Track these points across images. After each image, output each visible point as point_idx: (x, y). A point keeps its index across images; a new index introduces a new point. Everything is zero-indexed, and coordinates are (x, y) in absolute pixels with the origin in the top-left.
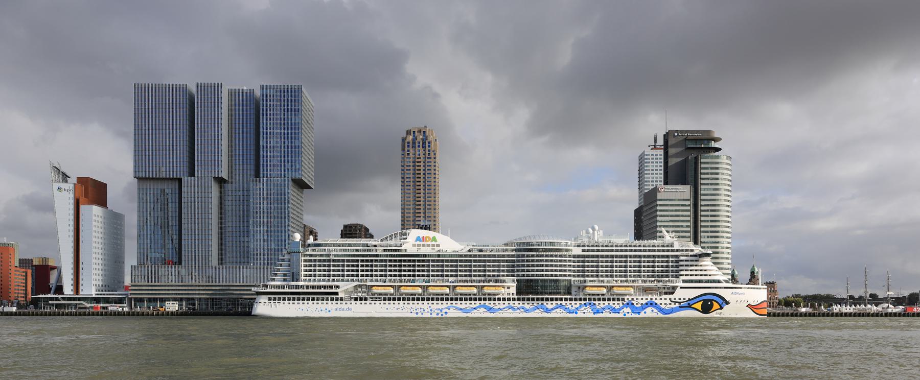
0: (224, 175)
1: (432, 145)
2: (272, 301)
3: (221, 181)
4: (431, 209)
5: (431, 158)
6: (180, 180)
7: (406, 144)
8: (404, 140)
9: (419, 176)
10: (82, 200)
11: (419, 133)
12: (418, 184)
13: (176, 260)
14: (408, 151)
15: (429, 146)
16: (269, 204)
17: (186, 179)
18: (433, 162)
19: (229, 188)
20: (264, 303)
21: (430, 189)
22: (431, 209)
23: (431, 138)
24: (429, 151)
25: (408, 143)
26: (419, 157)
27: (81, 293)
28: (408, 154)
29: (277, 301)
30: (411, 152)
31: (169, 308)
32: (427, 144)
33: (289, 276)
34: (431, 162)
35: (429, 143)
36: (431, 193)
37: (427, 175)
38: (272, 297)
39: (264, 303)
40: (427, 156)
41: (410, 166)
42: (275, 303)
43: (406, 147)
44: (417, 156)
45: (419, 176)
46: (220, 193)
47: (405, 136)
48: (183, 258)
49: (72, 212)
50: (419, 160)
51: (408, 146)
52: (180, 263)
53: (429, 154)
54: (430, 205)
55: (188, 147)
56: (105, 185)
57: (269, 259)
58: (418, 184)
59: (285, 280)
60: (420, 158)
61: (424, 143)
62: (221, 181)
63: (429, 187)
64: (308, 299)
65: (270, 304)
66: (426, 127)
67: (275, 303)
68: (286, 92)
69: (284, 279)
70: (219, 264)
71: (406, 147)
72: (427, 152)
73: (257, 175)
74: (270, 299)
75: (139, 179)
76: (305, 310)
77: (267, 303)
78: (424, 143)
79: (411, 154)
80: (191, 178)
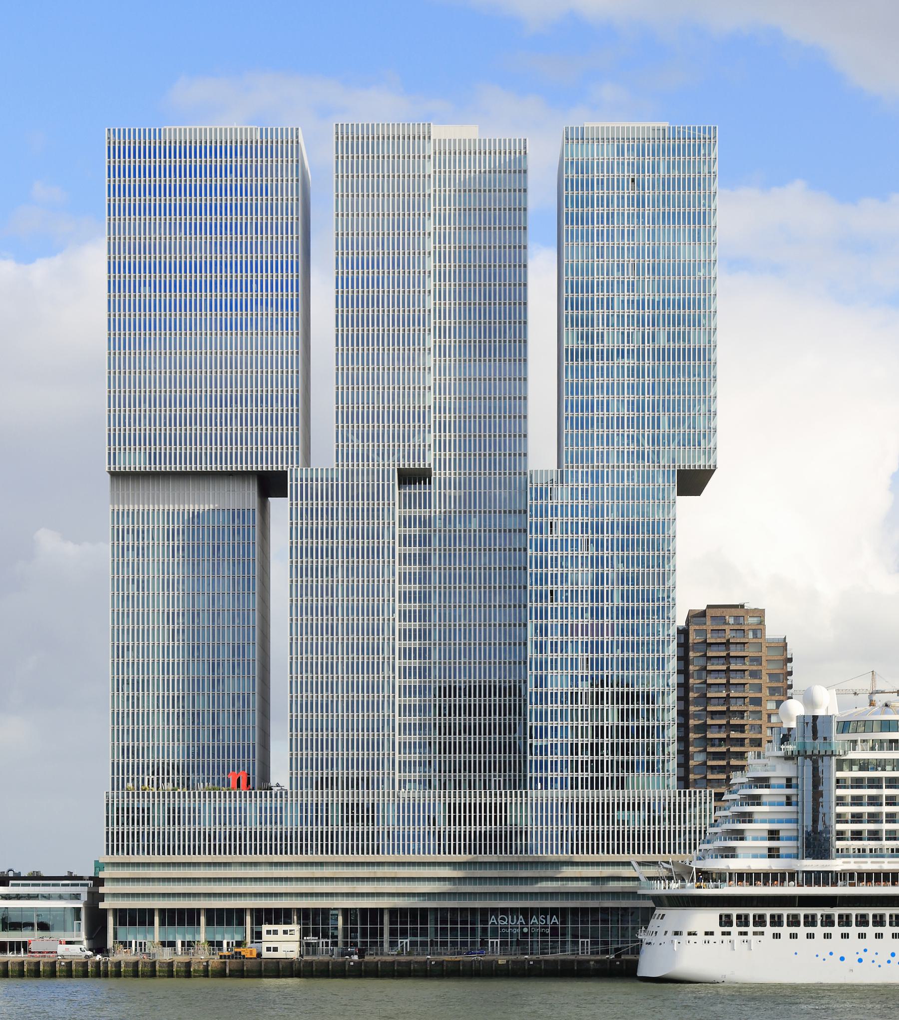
2: (735, 929)
20: (707, 933)
29: (751, 929)
31: (275, 949)
33: (789, 839)
38: (734, 912)
39: (707, 933)
42: (745, 933)
59: (773, 853)
64: (862, 921)
65: (726, 938)
67: (745, 933)
69: (770, 849)
74: (725, 921)
76: (851, 960)
77: (718, 936)
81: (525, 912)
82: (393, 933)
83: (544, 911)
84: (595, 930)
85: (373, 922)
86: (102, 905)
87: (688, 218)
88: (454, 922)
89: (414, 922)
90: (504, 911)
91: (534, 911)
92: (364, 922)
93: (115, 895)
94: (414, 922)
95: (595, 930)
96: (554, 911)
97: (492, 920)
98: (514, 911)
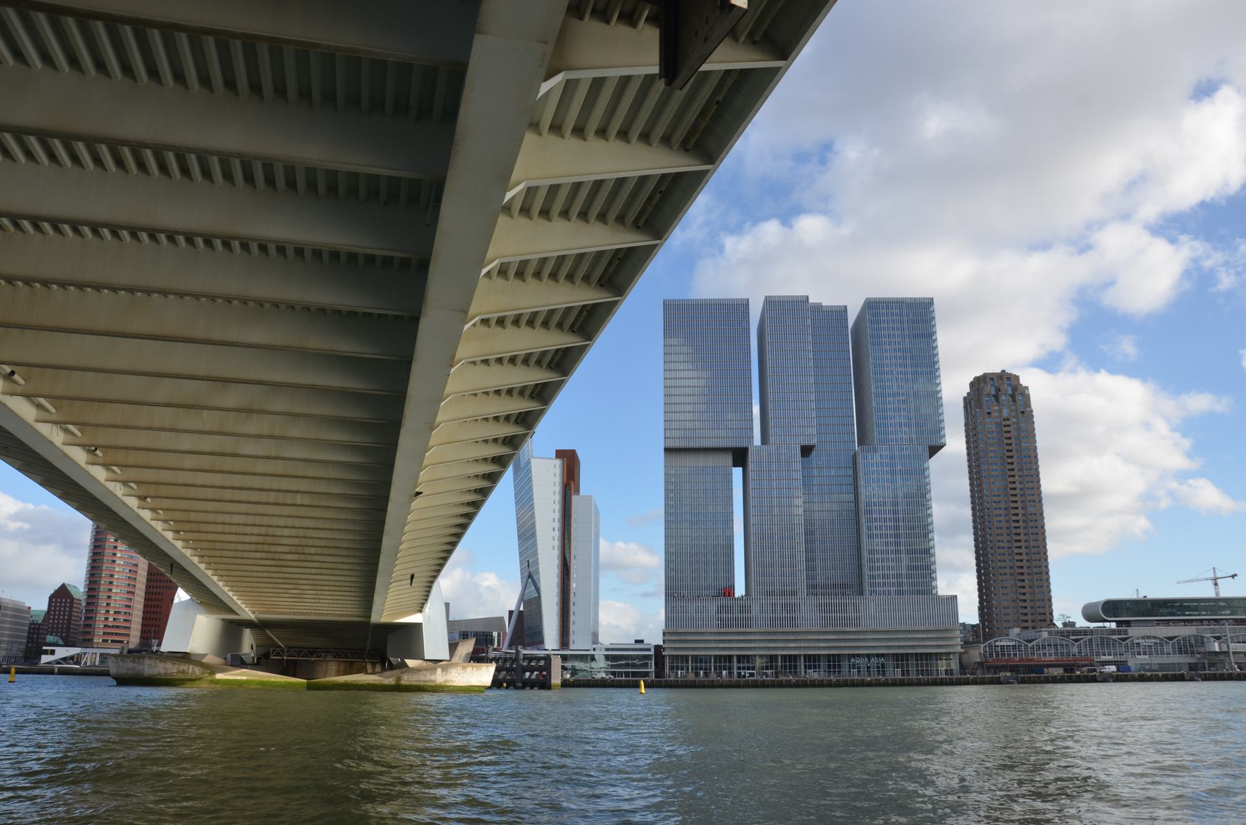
4: (1034, 501)
11: (1001, 382)
25: (988, 395)
27: (572, 646)
32: (1019, 398)
50: (1008, 423)
57: (900, 584)
60: (1008, 419)
61: (1013, 397)
78: (1013, 397)
81: (868, 656)
82: (805, 668)
83: (878, 655)
84: (902, 665)
85: (795, 661)
86: (664, 653)
87: (923, 336)
88: (834, 661)
89: (815, 661)
90: (858, 655)
91: (873, 655)
92: (790, 662)
94: (815, 661)
95: (902, 665)
96: (882, 655)
97: (852, 660)
98: (863, 655)
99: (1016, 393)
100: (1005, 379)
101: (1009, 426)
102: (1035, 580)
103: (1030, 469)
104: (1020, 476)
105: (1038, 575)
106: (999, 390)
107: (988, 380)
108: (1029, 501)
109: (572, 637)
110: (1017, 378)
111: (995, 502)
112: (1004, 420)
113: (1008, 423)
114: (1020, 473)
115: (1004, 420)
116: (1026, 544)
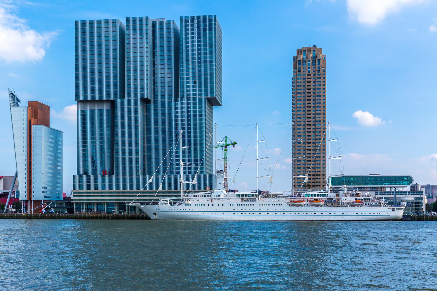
0: (149, 96)
1: (321, 62)
3: (145, 102)
4: (320, 121)
5: (320, 74)
6: (112, 102)
7: (298, 63)
8: (295, 59)
9: (309, 91)
10: (33, 120)
12: (308, 98)
13: (109, 170)
14: (300, 68)
15: (319, 64)
16: (187, 120)
17: (118, 100)
18: (322, 78)
19: (152, 107)
21: (320, 103)
22: (320, 121)
23: (320, 56)
24: (319, 68)
25: (300, 61)
26: (309, 74)
28: (299, 71)
30: (302, 69)
32: (317, 62)
34: (320, 78)
35: (319, 60)
36: (320, 107)
37: (316, 90)
40: (317, 73)
41: (301, 82)
43: (298, 65)
44: (307, 73)
45: (309, 91)
46: (145, 112)
47: (296, 55)
48: (116, 170)
49: (26, 131)
50: (310, 77)
51: (300, 65)
52: (112, 173)
53: (319, 71)
54: (320, 118)
55: (119, 73)
56: (49, 107)
58: (308, 98)
60: (310, 75)
61: (314, 61)
62: (145, 102)
63: (319, 101)
66: (315, 46)
68: (202, 22)
70: (145, 173)
71: (298, 65)
72: (317, 69)
73: (177, 94)
75: (78, 102)
78: (314, 61)
79: (302, 72)
80: (122, 100)
86: (72, 202)
93: (75, 200)
99: (317, 59)
100: (312, 51)
101: (310, 78)
102: (316, 164)
103: (320, 103)
104: (314, 107)
105: (319, 162)
106: (307, 58)
107: (302, 51)
108: (317, 121)
109: (33, 194)
110: (321, 50)
111: (298, 122)
112: (308, 75)
113: (310, 77)
114: (314, 105)
115: (308, 75)
116: (313, 145)
